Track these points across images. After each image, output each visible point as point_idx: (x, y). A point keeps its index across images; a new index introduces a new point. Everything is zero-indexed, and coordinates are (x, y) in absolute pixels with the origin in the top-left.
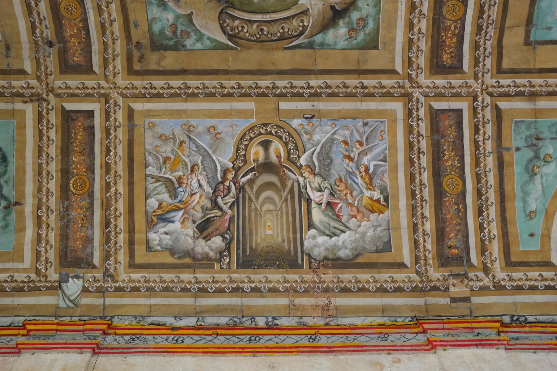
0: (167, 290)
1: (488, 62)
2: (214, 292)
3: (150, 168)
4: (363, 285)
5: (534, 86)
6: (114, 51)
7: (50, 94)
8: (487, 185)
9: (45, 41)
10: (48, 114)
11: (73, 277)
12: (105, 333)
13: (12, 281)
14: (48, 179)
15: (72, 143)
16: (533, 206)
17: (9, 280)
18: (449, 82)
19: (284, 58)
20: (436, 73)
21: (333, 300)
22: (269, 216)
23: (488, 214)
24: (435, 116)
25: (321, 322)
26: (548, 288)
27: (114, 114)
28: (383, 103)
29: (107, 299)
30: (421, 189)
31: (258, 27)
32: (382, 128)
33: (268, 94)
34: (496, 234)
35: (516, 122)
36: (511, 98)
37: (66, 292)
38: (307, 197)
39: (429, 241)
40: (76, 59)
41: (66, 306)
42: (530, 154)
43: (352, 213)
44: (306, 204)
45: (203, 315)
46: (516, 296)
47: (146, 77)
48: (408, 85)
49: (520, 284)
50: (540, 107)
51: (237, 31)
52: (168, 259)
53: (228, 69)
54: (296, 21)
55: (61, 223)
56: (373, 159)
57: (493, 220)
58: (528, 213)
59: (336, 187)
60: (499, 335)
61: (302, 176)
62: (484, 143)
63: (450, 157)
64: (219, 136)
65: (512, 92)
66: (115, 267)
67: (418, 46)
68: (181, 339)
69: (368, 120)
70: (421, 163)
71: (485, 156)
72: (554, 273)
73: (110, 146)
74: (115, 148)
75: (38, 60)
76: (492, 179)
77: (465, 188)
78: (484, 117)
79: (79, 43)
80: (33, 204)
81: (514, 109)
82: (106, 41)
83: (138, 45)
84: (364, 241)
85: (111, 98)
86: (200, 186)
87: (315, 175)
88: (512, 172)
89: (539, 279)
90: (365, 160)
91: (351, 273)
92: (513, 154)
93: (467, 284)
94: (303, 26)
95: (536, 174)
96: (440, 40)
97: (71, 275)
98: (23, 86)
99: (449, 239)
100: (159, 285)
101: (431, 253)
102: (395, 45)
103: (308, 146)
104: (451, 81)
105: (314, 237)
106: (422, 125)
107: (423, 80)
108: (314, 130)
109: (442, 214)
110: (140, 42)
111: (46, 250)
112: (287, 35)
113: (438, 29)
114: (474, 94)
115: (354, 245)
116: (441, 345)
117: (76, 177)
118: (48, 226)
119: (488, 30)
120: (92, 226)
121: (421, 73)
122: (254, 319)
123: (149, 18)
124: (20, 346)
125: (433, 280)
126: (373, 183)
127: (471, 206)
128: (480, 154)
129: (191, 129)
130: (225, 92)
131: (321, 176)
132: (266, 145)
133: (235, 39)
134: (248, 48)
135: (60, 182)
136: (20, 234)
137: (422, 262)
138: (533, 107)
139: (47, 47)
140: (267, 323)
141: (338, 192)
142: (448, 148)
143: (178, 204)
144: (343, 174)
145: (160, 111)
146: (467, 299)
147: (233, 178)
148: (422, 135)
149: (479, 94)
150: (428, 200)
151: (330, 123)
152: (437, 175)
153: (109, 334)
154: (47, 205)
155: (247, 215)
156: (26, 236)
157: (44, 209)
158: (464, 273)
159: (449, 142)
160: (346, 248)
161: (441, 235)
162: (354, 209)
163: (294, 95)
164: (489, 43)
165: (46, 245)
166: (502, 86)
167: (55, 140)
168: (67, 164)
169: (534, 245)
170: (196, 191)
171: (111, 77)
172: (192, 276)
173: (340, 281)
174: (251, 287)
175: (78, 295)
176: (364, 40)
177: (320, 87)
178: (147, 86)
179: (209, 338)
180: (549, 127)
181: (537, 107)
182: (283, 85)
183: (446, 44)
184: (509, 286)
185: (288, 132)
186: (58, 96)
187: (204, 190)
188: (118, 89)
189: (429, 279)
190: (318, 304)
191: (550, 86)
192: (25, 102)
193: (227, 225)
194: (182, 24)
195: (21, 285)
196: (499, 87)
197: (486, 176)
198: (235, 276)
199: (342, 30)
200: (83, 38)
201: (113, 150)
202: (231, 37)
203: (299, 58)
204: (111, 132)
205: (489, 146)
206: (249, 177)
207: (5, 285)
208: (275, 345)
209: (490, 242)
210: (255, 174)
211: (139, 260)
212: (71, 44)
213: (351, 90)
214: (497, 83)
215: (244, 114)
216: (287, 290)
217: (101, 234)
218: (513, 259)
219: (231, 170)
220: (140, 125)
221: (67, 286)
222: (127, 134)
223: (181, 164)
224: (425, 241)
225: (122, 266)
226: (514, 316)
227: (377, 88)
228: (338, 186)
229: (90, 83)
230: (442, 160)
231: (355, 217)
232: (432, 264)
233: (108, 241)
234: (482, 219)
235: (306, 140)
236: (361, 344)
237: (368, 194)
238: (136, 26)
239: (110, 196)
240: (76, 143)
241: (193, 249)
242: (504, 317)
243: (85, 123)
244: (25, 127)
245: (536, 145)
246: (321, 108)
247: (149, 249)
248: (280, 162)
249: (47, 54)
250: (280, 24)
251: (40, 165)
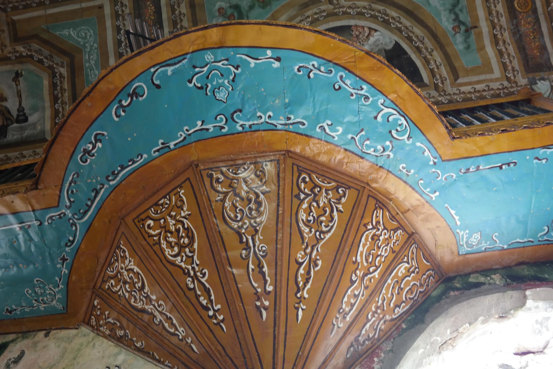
11: (539, 80)
13: (489, 90)
14: (494, 4)
17: (486, 89)
80: (488, 26)
97: (537, 78)
111: (510, 60)
118: (504, 42)
154: (500, 25)
156: (488, 52)
157: (498, 28)
175: (550, 93)
195: (498, 92)
207: (484, 94)
221: (538, 87)
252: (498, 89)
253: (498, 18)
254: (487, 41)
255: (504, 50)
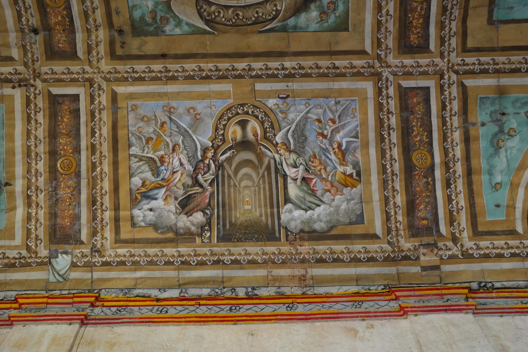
0: (151, 263)
1: (453, 41)
2: (196, 264)
3: (133, 148)
4: (338, 256)
5: (498, 64)
6: (97, 37)
7: (37, 79)
8: (454, 158)
9: (31, 28)
10: (35, 98)
11: (62, 253)
12: (93, 305)
14: (36, 160)
15: (58, 126)
16: (498, 178)
18: (417, 62)
19: (258, 42)
20: (404, 53)
21: (309, 270)
22: (247, 192)
23: (456, 187)
24: (404, 94)
25: (298, 291)
26: (513, 255)
27: (99, 97)
28: (354, 82)
29: (94, 273)
30: (391, 164)
31: (233, 12)
32: (353, 107)
33: (244, 75)
34: (464, 206)
35: (481, 98)
36: (476, 75)
37: (56, 267)
38: (284, 173)
39: (400, 212)
40: (61, 46)
41: (55, 281)
42: (494, 128)
43: (326, 188)
44: (282, 180)
45: (186, 286)
46: (483, 264)
47: (127, 62)
48: (377, 64)
49: (487, 252)
50: (504, 84)
51: (213, 16)
52: (153, 235)
53: (206, 52)
54: (269, 5)
55: (49, 202)
56: (346, 136)
57: (461, 192)
58: (494, 185)
59: (310, 163)
60: (467, 301)
61: (278, 153)
62: (451, 119)
63: (418, 133)
64: (198, 117)
65: (477, 70)
66: (102, 243)
67: (386, 27)
68: (165, 309)
69: (340, 99)
70: (392, 139)
71: (452, 131)
72: (519, 241)
73: (95, 128)
74: (100, 130)
75: (24, 47)
76: (459, 152)
77: (434, 162)
78: (450, 93)
79: (63, 30)
80: (23, 185)
81: (479, 87)
82: (89, 28)
83: (121, 32)
84: (338, 214)
85: (95, 82)
86: (181, 164)
87: (290, 152)
88: (478, 146)
89: (505, 247)
90: (338, 137)
91: (326, 244)
92: (479, 129)
93: (437, 253)
94: (277, 10)
95: (501, 148)
96: (408, 21)
97: (60, 251)
98: (11, 73)
99: (419, 211)
100: (144, 259)
101: (402, 225)
102: (364, 27)
103: (283, 124)
104: (419, 60)
105: (290, 211)
106: (392, 103)
107: (392, 60)
108: (289, 109)
109: (412, 187)
110: (122, 29)
111: (36, 227)
112: (261, 19)
113: (405, 10)
114: (441, 72)
115: (328, 218)
116: (412, 311)
117: (63, 158)
118: (37, 205)
119: (453, 11)
120: (79, 204)
121: (390, 54)
122: (235, 290)
123: (130, 5)
124: (12, 319)
125: (404, 250)
126: (346, 158)
127: (440, 179)
128: (447, 129)
129: (172, 110)
130: (204, 75)
131: (296, 153)
132: (243, 124)
133: (212, 24)
134: (225, 32)
135: (48, 163)
136: (11, 213)
137: (394, 233)
138: (497, 84)
139: (32, 34)
140: (247, 293)
141: (312, 168)
142: (417, 124)
143: (160, 182)
144: (317, 150)
145: (142, 93)
146: (437, 268)
147: (212, 156)
148: (392, 112)
149: (445, 72)
150: (398, 174)
151: (304, 102)
152: (407, 150)
153: (97, 306)
154: (36, 186)
155: (226, 191)
156: (17, 215)
157: (33, 188)
158: (433, 242)
159: (417, 118)
160: (321, 221)
161: (411, 207)
162: (328, 184)
163: (269, 76)
164: (454, 24)
165: (36, 222)
166: (467, 65)
167: (42, 123)
168: (54, 146)
169: (500, 216)
170: (178, 169)
171: (95, 63)
172: (175, 250)
173: (315, 252)
174: (231, 259)
175: (67, 270)
176: (334, 22)
177: (294, 68)
178: (129, 70)
179: (192, 308)
180: (513, 103)
181: (501, 84)
182: (259, 67)
183: (413, 25)
184: (477, 255)
185: (264, 112)
186: (44, 81)
187: (185, 168)
188: (101, 74)
189: (401, 249)
190: (295, 275)
191: (513, 63)
192: (14, 87)
193: (207, 201)
194: (162, 11)
195: (12, 261)
196: (464, 65)
197: (453, 150)
198: (216, 249)
199: (314, 14)
200: (68, 25)
201: (98, 131)
202: (207, 22)
203: (273, 42)
204: (96, 114)
205: (456, 121)
206: (228, 155)
208: (254, 313)
209: (458, 213)
210: (233, 152)
211: (124, 236)
212: (56, 31)
213: (324, 71)
214: (462, 62)
215: (221, 95)
216: (265, 262)
217: (88, 211)
218: (480, 229)
219: (211, 148)
220: (123, 108)
221: (56, 261)
222: (111, 116)
223: (162, 144)
224: (396, 213)
225: (109, 241)
226: (481, 282)
227: (348, 68)
228: (312, 162)
229: (75, 68)
230: (411, 136)
231: (329, 191)
232: (403, 235)
233: (94, 218)
234: (450, 191)
235: (281, 119)
236: (336, 311)
237: (341, 169)
238: (118, 13)
239: (96, 176)
240: (63, 126)
241: (175, 224)
242: (472, 284)
243: (71, 106)
244: (14, 112)
245: (500, 120)
246: (295, 88)
247: (134, 225)
248: (257, 140)
249: (33, 41)
250: (255, 9)
251: (29, 147)
252: (15, 258)
253: (36, 177)
254: (20, 202)
255: (33, 214)
